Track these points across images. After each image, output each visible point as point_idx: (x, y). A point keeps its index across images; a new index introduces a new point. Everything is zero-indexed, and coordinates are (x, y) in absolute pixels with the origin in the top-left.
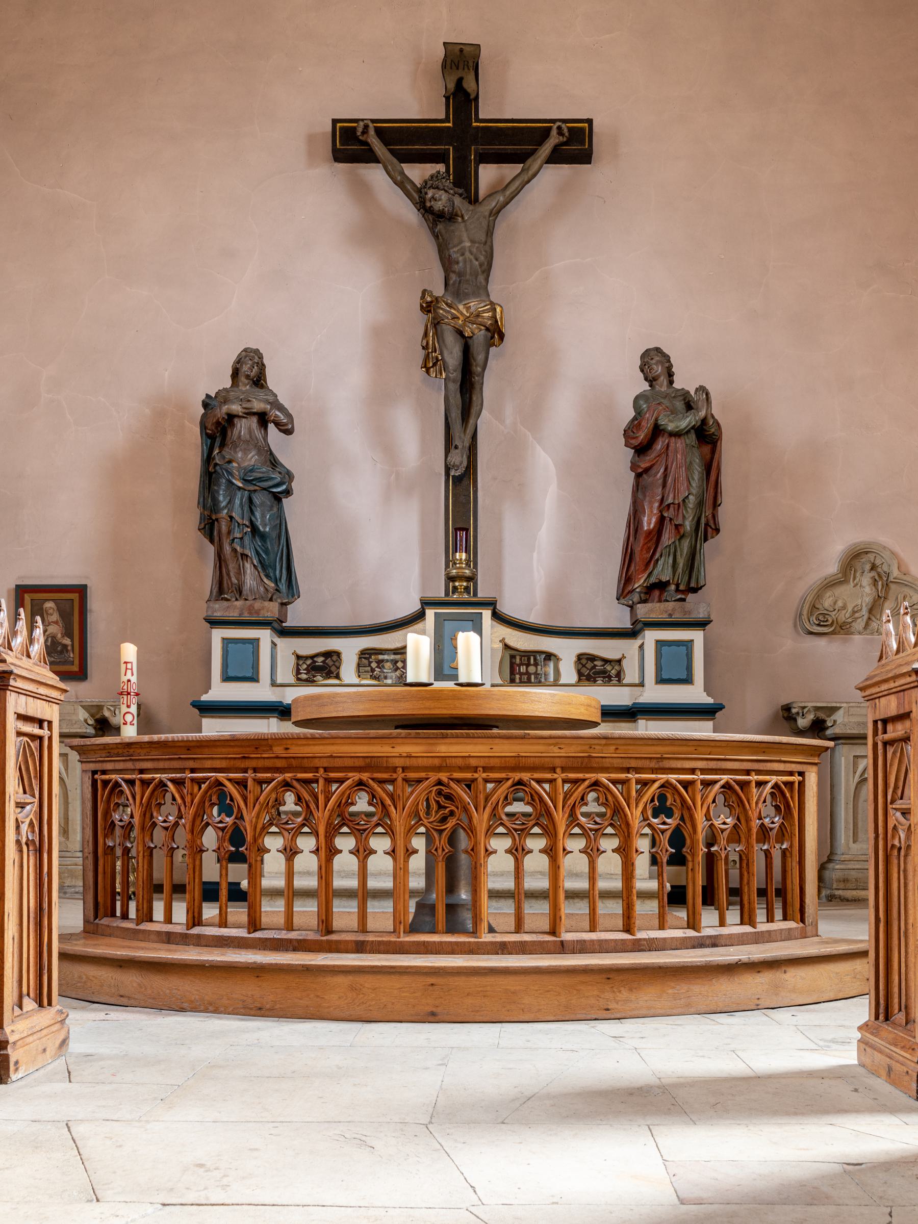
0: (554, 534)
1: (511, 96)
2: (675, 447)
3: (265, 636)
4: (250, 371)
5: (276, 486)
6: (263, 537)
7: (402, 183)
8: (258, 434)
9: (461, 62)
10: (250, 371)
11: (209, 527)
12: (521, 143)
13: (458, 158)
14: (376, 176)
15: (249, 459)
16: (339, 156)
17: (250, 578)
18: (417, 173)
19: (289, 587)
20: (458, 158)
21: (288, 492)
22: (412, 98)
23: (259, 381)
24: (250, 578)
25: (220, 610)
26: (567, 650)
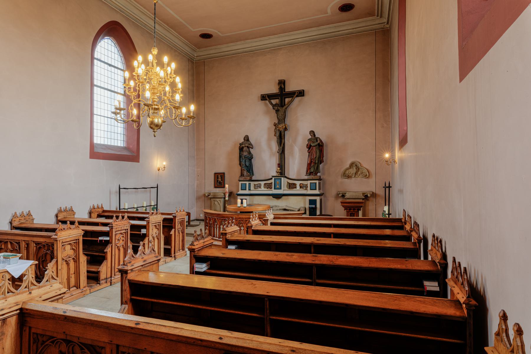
0: (297, 162)
1: (290, 87)
2: (317, 148)
3: (247, 183)
4: (247, 139)
5: (250, 158)
6: (247, 166)
7: (271, 104)
8: (247, 149)
9: (282, 83)
10: (247, 139)
11: (240, 164)
12: (293, 95)
13: (281, 99)
14: (267, 102)
15: (245, 154)
16: (262, 100)
17: (245, 173)
18: (274, 102)
19: (253, 174)
20: (281, 99)
21: (252, 158)
22: (274, 90)
23: (248, 140)
24: (245, 173)
25: (241, 179)
26: (298, 183)
